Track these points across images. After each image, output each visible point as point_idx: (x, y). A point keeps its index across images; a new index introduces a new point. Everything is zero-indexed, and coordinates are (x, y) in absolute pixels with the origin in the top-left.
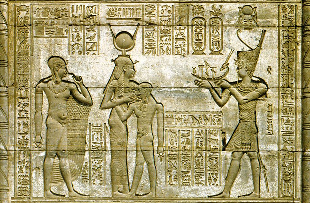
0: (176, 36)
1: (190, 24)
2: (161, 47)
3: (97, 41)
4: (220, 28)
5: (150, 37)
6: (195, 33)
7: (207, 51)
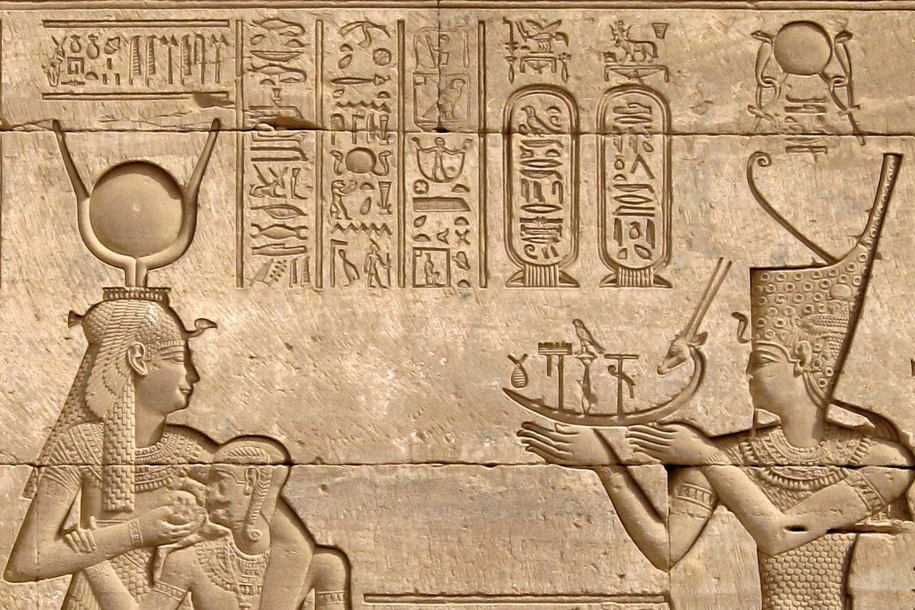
0: (421, 187)
1: (495, 122)
2: (338, 247)
4: (658, 141)
5: (279, 191)
6: (523, 172)
7: (590, 267)
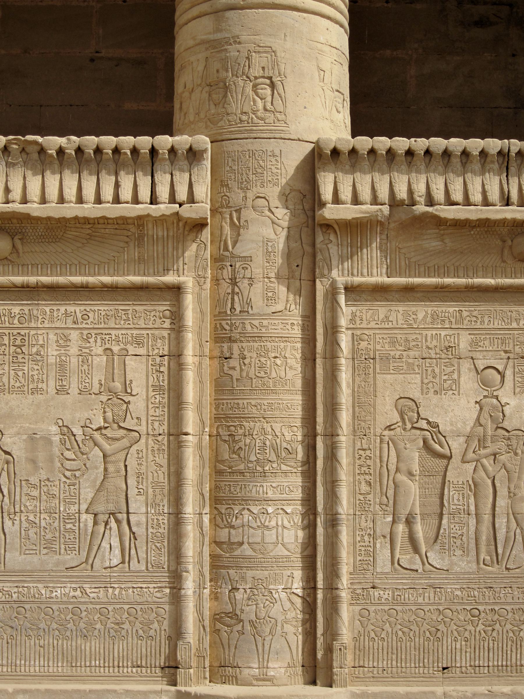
3: (456, 378)
